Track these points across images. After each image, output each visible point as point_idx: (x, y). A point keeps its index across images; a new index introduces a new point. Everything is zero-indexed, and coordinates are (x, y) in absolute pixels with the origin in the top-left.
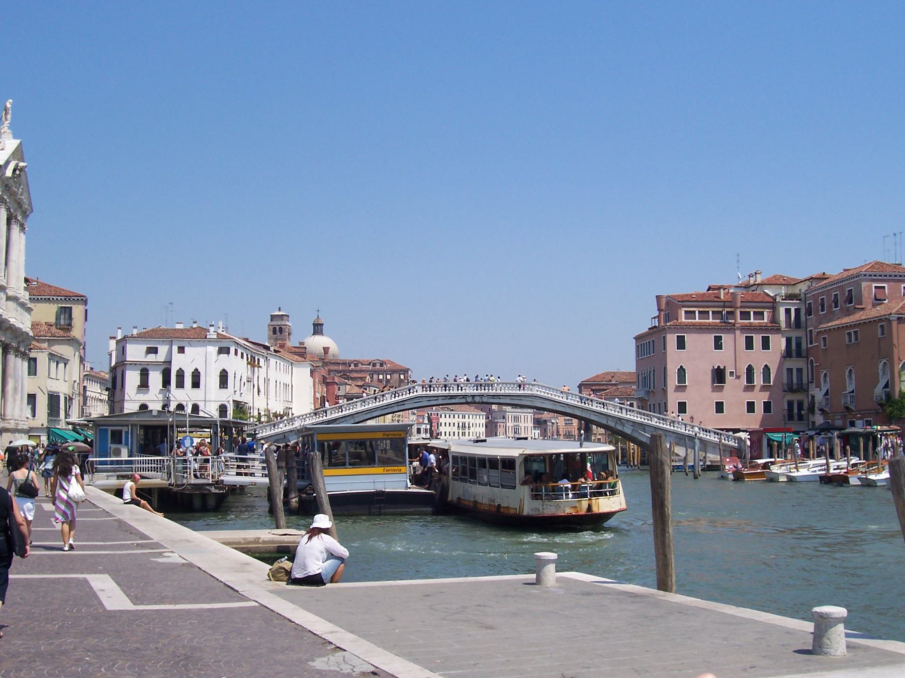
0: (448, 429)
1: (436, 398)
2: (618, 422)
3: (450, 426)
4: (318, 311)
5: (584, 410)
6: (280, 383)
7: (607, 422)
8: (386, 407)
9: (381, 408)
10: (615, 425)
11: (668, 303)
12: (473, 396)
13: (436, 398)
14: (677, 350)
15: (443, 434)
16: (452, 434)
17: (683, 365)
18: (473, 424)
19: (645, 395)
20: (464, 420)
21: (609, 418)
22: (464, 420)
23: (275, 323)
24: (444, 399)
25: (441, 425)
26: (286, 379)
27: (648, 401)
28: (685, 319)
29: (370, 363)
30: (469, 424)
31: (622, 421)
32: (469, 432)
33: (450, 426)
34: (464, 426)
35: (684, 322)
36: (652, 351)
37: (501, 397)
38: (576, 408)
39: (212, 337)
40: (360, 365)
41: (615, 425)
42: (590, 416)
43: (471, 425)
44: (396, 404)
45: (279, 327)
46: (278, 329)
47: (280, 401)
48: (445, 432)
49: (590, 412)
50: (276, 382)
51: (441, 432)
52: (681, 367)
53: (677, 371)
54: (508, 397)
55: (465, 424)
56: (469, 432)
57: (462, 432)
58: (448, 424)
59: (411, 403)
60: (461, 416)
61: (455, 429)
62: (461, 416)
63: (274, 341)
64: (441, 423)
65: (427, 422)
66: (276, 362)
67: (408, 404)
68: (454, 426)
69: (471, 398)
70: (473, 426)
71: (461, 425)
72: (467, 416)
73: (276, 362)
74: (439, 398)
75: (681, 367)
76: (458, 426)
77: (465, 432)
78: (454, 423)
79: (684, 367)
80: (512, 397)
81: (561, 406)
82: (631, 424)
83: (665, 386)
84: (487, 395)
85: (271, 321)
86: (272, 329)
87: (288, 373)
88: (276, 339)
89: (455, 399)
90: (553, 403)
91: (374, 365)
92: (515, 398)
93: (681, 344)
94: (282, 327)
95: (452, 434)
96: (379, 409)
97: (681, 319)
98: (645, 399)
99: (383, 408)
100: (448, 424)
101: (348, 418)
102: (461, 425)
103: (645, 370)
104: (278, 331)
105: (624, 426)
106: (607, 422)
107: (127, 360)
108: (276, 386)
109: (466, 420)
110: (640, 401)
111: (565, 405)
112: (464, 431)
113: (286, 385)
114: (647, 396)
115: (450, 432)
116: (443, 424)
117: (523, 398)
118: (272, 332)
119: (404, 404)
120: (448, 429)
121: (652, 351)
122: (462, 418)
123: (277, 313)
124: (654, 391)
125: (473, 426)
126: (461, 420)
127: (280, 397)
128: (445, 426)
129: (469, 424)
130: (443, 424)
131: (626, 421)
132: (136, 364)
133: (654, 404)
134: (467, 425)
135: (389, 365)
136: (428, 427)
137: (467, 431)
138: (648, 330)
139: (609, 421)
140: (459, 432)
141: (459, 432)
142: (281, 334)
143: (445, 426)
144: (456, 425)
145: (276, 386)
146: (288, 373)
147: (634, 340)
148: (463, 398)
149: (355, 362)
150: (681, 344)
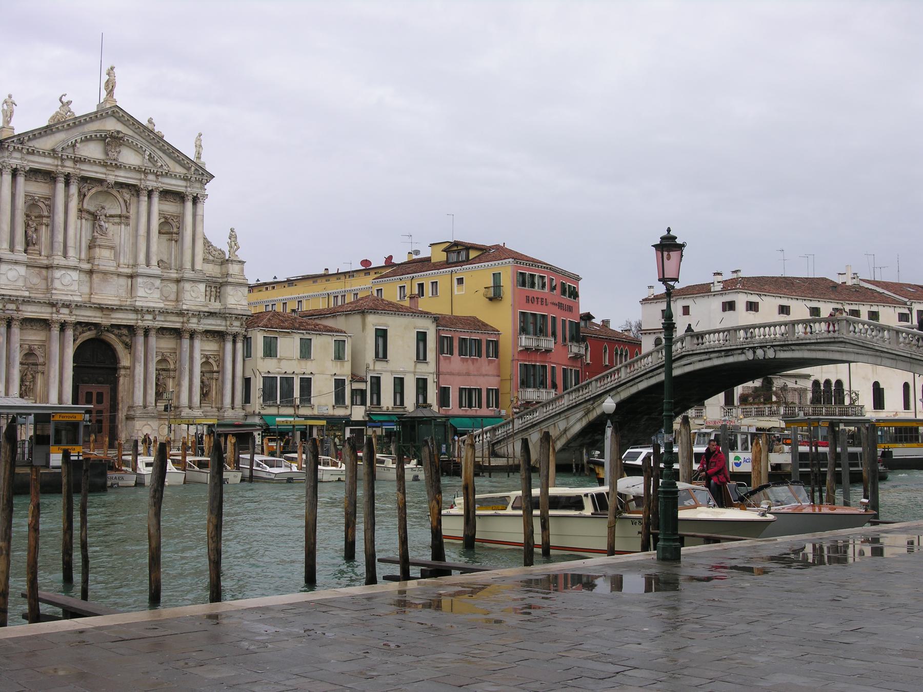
1: (707, 357)
8: (651, 374)
12: (754, 349)
24: (719, 357)
37: (793, 347)
69: (751, 351)
74: (712, 355)
80: (808, 347)
84: (772, 346)
89: (732, 355)
92: (813, 347)
96: (643, 378)
111: (894, 357)
148: (743, 353)
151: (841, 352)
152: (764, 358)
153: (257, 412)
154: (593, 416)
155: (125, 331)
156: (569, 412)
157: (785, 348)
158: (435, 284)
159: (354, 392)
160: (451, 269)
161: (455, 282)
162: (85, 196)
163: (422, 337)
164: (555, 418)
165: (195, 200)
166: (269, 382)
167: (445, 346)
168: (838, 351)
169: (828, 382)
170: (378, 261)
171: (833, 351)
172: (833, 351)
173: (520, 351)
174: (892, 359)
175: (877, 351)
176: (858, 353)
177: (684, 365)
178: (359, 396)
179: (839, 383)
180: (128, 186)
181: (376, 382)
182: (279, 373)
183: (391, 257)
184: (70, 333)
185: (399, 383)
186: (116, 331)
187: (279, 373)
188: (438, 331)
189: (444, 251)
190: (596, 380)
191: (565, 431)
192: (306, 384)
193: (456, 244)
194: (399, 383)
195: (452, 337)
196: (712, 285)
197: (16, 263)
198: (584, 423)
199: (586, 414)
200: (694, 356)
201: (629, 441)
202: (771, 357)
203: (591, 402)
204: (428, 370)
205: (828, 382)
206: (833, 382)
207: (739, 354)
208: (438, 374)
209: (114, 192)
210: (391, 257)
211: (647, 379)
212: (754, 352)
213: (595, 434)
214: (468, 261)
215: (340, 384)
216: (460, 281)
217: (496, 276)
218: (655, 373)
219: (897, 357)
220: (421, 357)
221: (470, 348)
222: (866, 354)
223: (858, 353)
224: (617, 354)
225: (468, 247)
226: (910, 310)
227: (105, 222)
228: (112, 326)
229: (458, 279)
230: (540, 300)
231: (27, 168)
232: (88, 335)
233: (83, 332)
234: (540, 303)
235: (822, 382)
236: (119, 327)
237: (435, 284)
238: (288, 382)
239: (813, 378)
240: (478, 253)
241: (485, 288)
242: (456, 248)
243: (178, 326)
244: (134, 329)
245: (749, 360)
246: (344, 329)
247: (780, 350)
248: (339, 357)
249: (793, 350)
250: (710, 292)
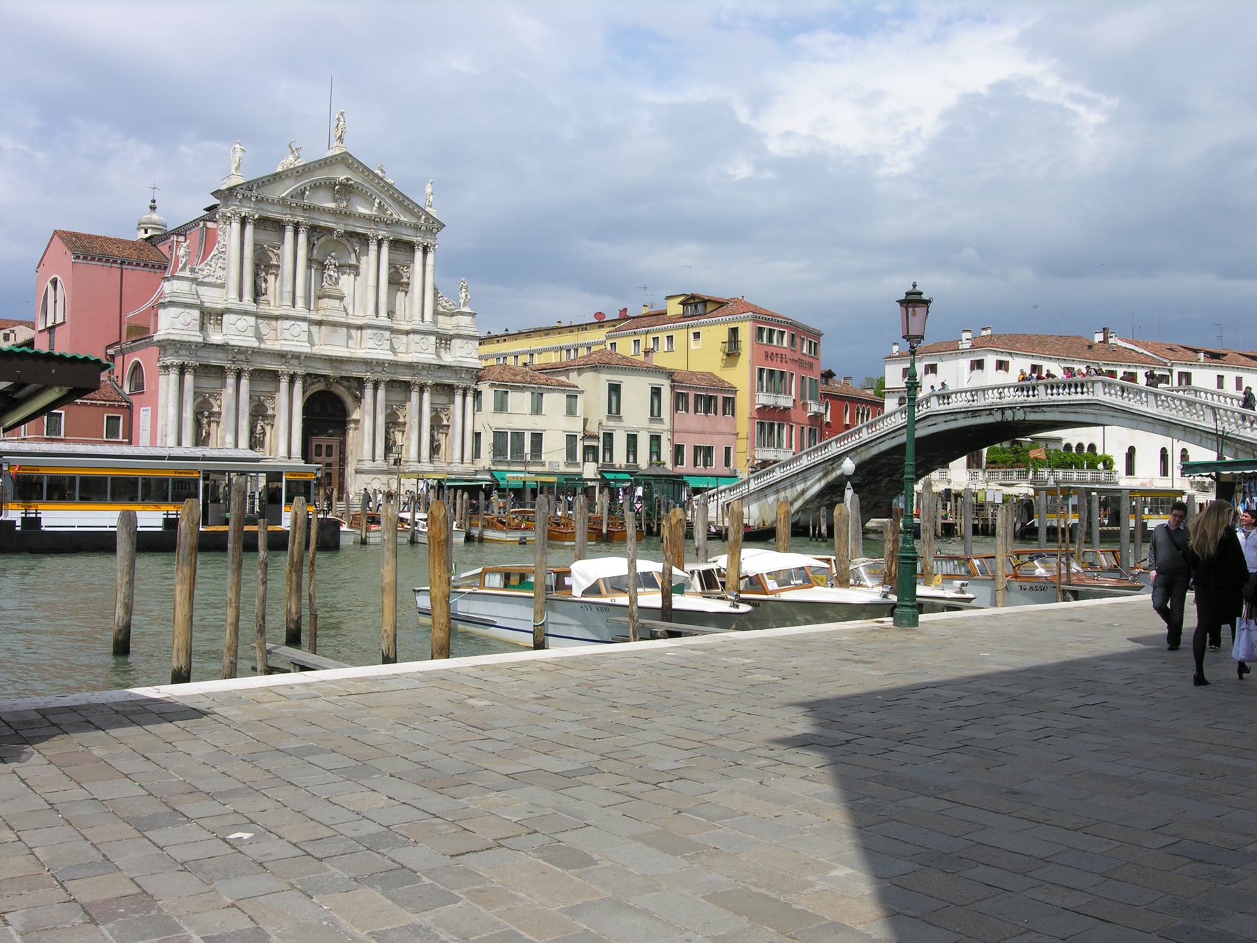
1: (953, 417)
5: (1187, 430)
8: (893, 435)
12: (1002, 410)
13: (953, 417)
37: (1044, 409)
39: (964, 348)
54: (1055, 409)
59: (923, 427)
74: (959, 416)
80: (1061, 409)
84: (1022, 407)
90: (1130, 416)
92: (1065, 409)
107: (886, 387)
111: (1150, 420)
117: (1078, 410)
132: (893, 392)
151: (1095, 414)
152: (1013, 419)
153: (487, 468)
154: (831, 477)
155: (355, 384)
156: (807, 473)
157: (1036, 410)
158: (670, 338)
159: (586, 448)
160: (687, 323)
161: (692, 336)
162: (314, 244)
163: (656, 392)
164: (793, 479)
165: (425, 250)
166: (499, 435)
167: (679, 400)
168: (1092, 414)
169: (1080, 446)
170: (612, 314)
171: (1086, 413)
172: (1086, 413)
173: (758, 409)
174: (1149, 423)
175: (1133, 414)
176: (1113, 416)
177: (929, 426)
178: (591, 452)
179: (1092, 447)
180: (358, 234)
181: (609, 437)
182: (510, 429)
183: (625, 310)
184: (298, 386)
185: (632, 440)
186: (346, 384)
187: (510, 429)
188: (673, 388)
189: (680, 303)
190: (836, 440)
191: (803, 492)
192: (537, 438)
193: (693, 297)
194: (632, 440)
195: (688, 394)
196: (960, 342)
197: (246, 313)
198: (823, 483)
199: (825, 475)
201: (869, 503)
202: (1021, 419)
203: (830, 463)
204: (663, 428)
205: (1080, 446)
206: (1086, 446)
207: (987, 415)
208: (673, 432)
209: (344, 241)
210: (625, 310)
211: (889, 439)
212: (1003, 413)
213: (834, 496)
214: (704, 315)
215: (571, 438)
216: (697, 335)
217: (734, 331)
218: (898, 433)
219: (1155, 421)
220: (655, 415)
221: (708, 404)
222: (1122, 418)
223: (1113, 416)
224: (858, 413)
225: (705, 302)
226: (1171, 371)
227: (334, 272)
228: (342, 378)
229: (694, 334)
230: (779, 356)
231: (256, 216)
232: (319, 387)
233: (313, 384)
234: (779, 359)
235: (1074, 446)
236: (348, 379)
237: (670, 338)
238: (518, 435)
239: (1064, 442)
240: (714, 307)
241: (723, 343)
242: (692, 301)
243: (407, 378)
244: (363, 382)
245: (998, 422)
246: (576, 384)
247: (1030, 412)
248: (571, 412)
249: (1044, 412)
250: (959, 350)
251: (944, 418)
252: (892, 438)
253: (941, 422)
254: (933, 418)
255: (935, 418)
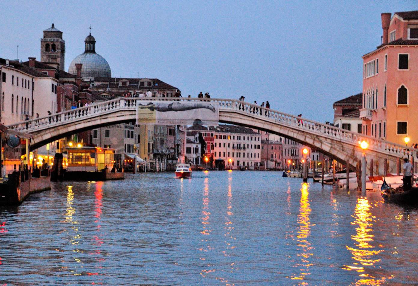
0: (222, 150)
2: (316, 139)
3: (224, 146)
4: (90, 28)
6: (17, 97)
7: (305, 139)
9: (84, 121)
10: (314, 143)
11: (395, 21)
14: (399, 70)
15: (218, 154)
16: (226, 154)
17: (404, 85)
18: (248, 145)
19: (369, 115)
20: (239, 141)
21: (307, 135)
22: (239, 141)
23: (48, 39)
25: (216, 146)
26: (26, 93)
27: (371, 120)
28: (410, 38)
29: (138, 81)
30: (244, 145)
31: (321, 138)
32: (244, 153)
33: (224, 146)
34: (239, 147)
35: (408, 41)
36: (376, 71)
38: (273, 124)
40: (128, 84)
41: (314, 143)
42: (288, 133)
43: (246, 146)
44: (99, 118)
45: (52, 43)
46: (51, 45)
47: (17, 115)
48: (220, 153)
49: (288, 129)
50: (13, 96)
51: (216, 153)
52: (403, 87)
53: (398, 91)
55: (240, 145)
56: (244, 153)
57: (237, 153)
58: (222, 145)
60: (236, 138)
61: (230, 150)
62: (236, 138)
63: (47, 58)
64: (216, 144)
65: (198, 142)
66: (13, 76)
67: (110, 117)
68: (229, 147)
70: (248, 148)
71: (236, 145)
72: (242, 138)
73: (13, 76)
75: (403, 87)
76: (233, 147)
77: (240, 153)
78: (229, 144)
79: (405, 87)
81: (260, 122)
82: (329, 141)
83: (385, 106)
85: (44, 37)
86: (45, 46)
87: (29, 88)
88: (49, 56)
90: (252, 119)
91: (142, 83)
93: (404, 62)
94: (56, 43)
95: (226, 154)
96: (82, 121)
97: (407, 38)
98: (368, 119)
99: (87, 121)
100: (222, 145)
101: (51, 130)
102: (236, 145)
103: (370, 91)
104: (51, 48)
105: (322, 143)
106: (305, 139)
108: (13, 99)
109: (242, 142)
110: (365, 122)
111: (264, 122)
112: (239, 152)
113: (24, 100)
114: (370, 115)
115: (224, 153)
116: (218, 145)
118: (44, 49)
119: (107, 118)
120: (222, 150)
121: (376, 71)
122: (238, 139)
123: (50, 30)
124: (376, 111)
125: (248, 148)
126: (236, 142)
127: (17, 112)
128: (220, 146)
129: (244, 145)
130: (218, 145)
131: (324, 139)
133: (376, 125)
134: (242, 146)
135: (157, 85)
136: (199, 146)
137: (242, 152)
138: (376, 48)
139: (307, 138)
140: (233, 153)
141: (233, 153)
142: (55, 50)
143: (220, 146)
144: (231, 146)
145: (13, 99)
146: (29, 88)
147: (363, 59)
149: (124, 80)
150: (404, 62)
168: (230, 117)
174: (262, 123)
176: (241, 119)
177: (118, 116)
200: (126, 112)
211: (84, 123)
218: (93, 119)
219: (265, 122)
222: (246, 119)
251: (131, 113)
252: (87, 122)
253: (127, 115)
254: (122, 112)
255: (124, 112)
